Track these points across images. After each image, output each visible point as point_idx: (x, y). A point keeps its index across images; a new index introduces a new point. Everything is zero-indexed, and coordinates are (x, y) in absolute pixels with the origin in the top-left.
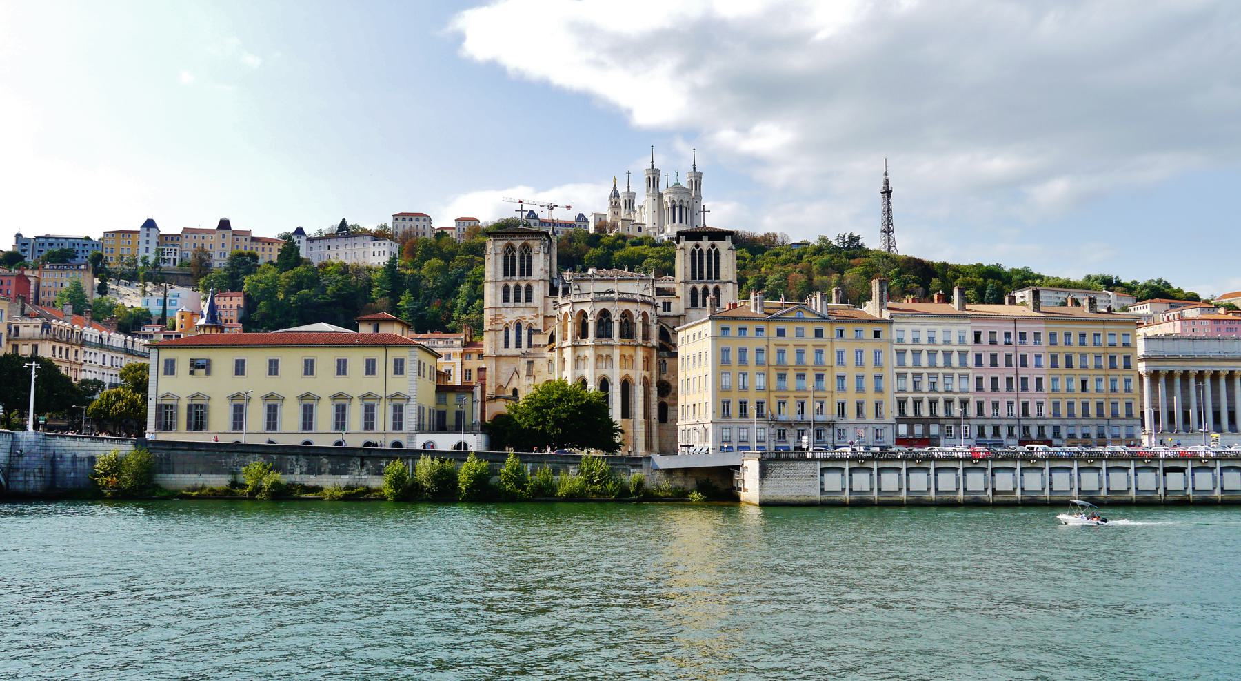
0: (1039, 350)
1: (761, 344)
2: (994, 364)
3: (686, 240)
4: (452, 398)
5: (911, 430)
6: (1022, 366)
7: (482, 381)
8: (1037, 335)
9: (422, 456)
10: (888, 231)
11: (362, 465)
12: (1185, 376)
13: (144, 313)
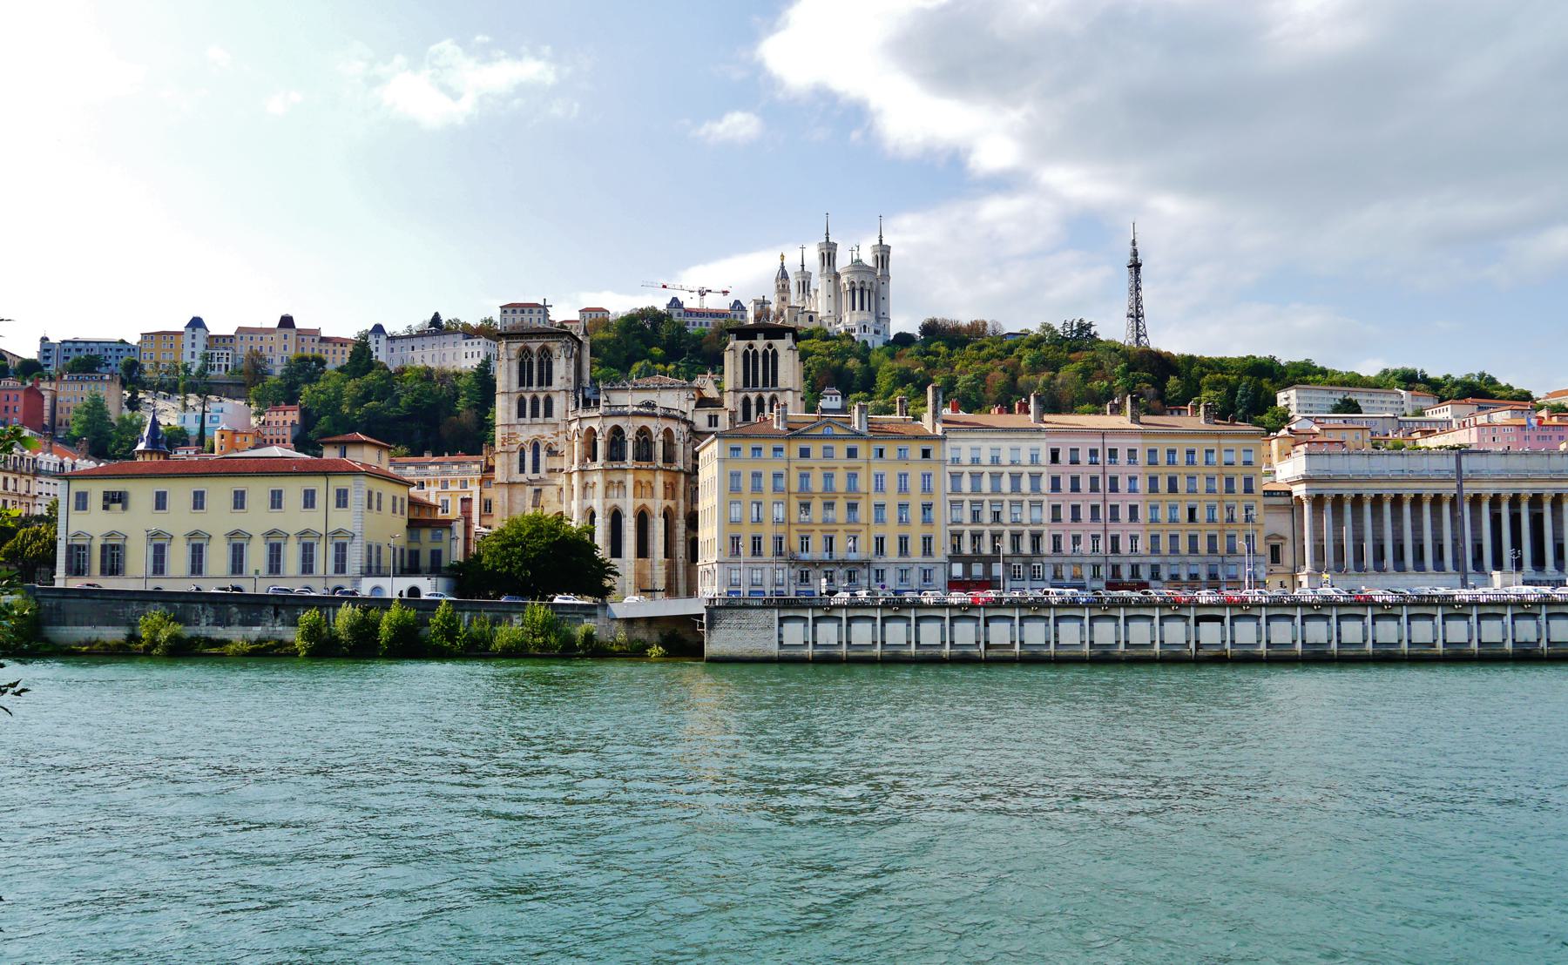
0: (1133, 470)
1: (780, 467)
2: (1075, 488)
3: (737, 339)
4: (426, 534)
5: (967, 570)
6: (1111, 491)
7: (467, 514)
8: (1132, 452)
9: (344, 604)
10: (1137, 316)
11: (276, 615)
12: (1358, 500)
13: (179, 432)
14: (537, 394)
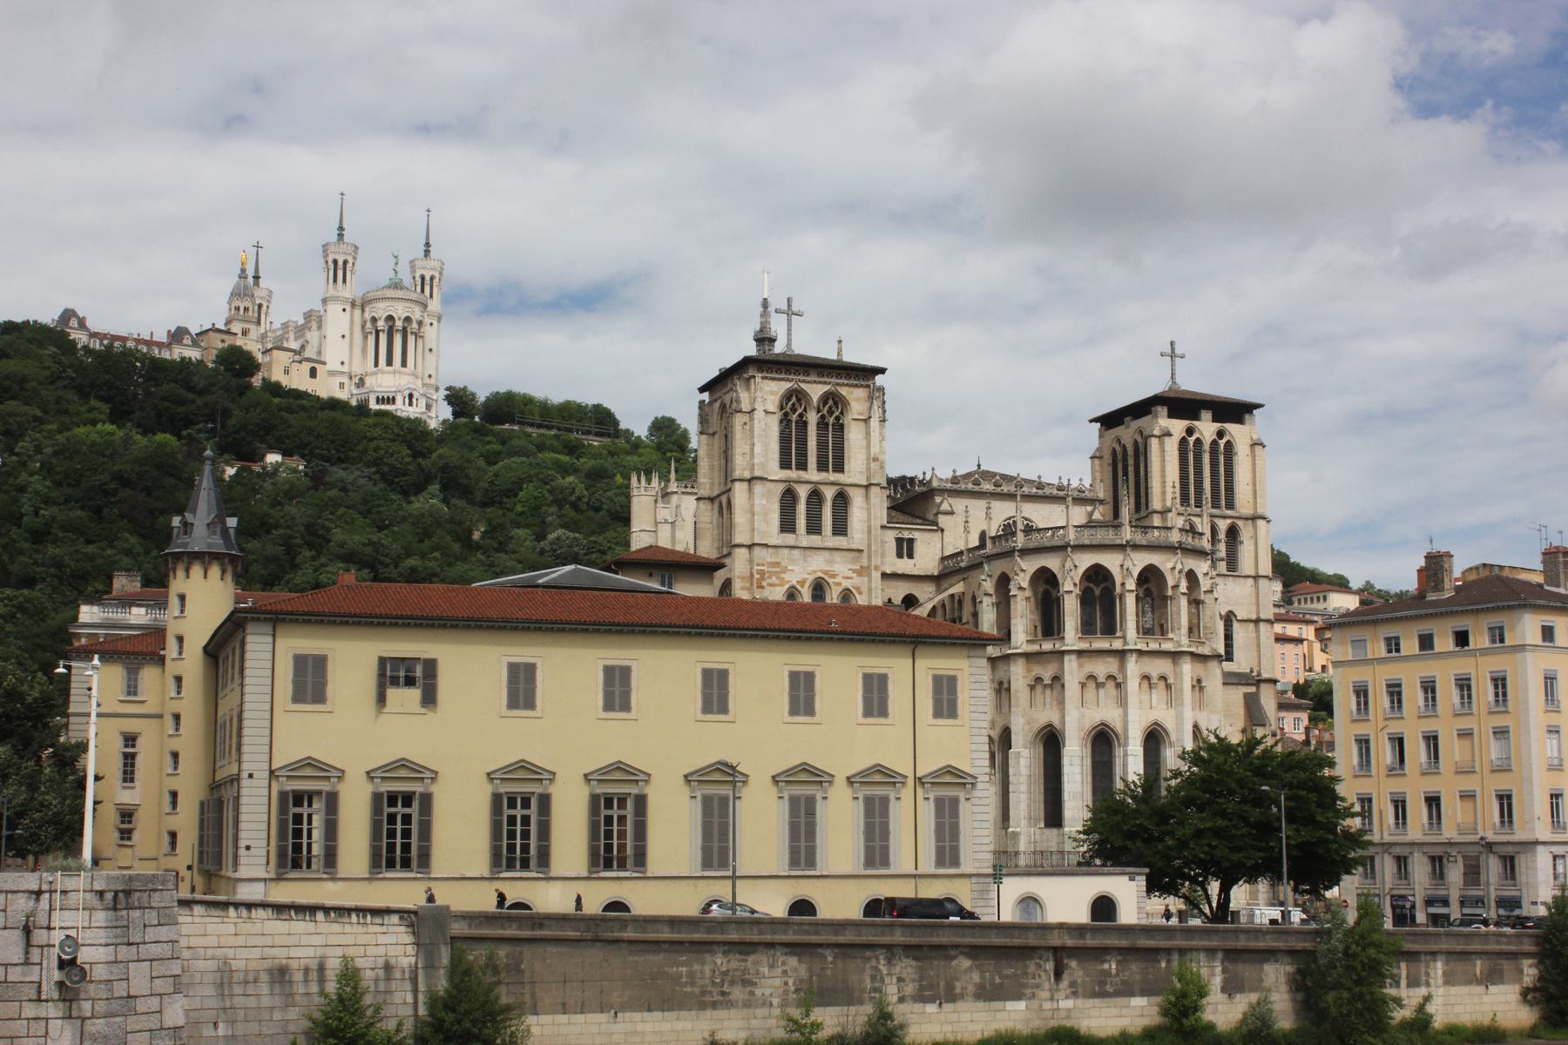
3: (1171, 416)
11: (1058, 975)
14: (823, 488)
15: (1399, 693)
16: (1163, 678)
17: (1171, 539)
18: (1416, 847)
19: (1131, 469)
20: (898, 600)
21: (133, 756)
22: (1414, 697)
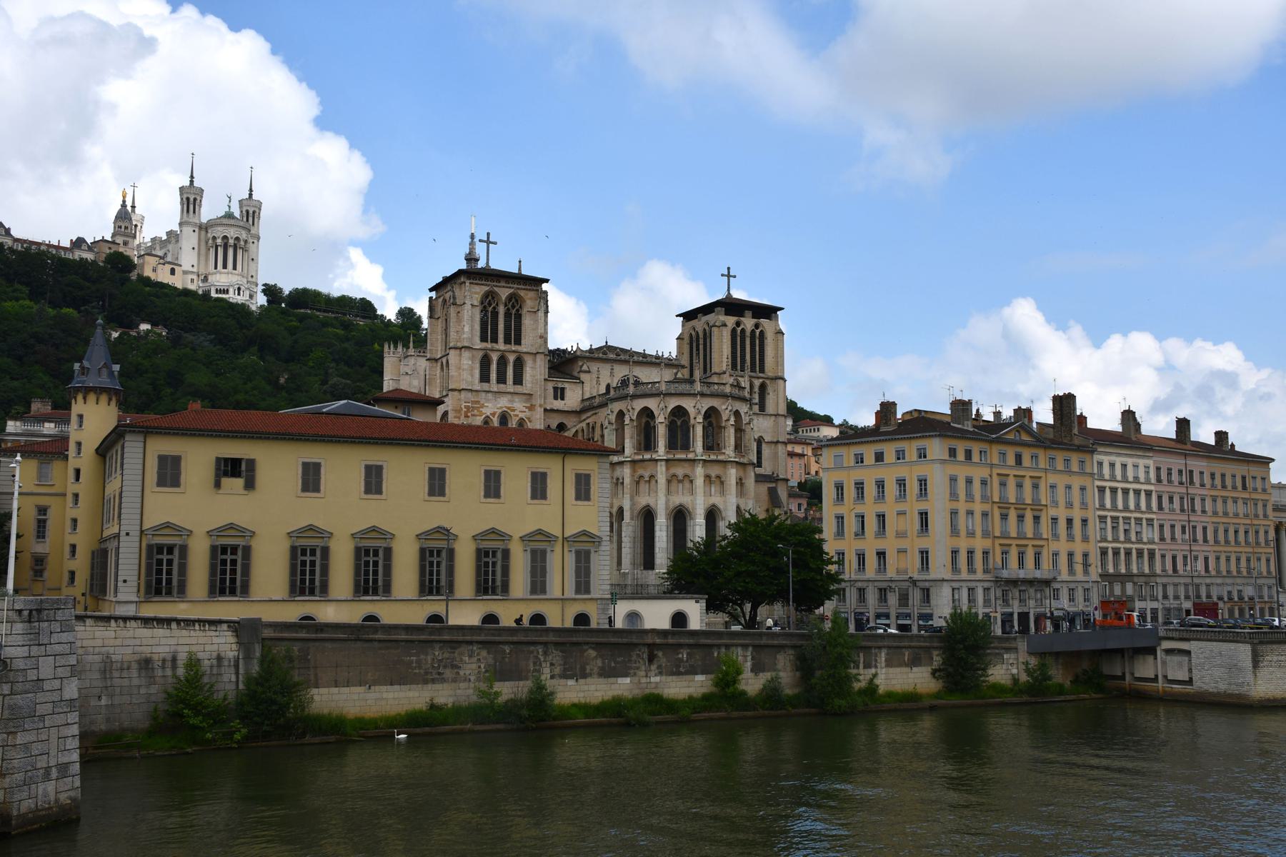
3: (726, 314)
14: (507, 354)
15: (863, 488)
16: (718, 477)
17: (726, 391)
18: (870, 583)
19: (701, 347)
20: (554, 426)
21: (45, 521)
22: (870, 490)
